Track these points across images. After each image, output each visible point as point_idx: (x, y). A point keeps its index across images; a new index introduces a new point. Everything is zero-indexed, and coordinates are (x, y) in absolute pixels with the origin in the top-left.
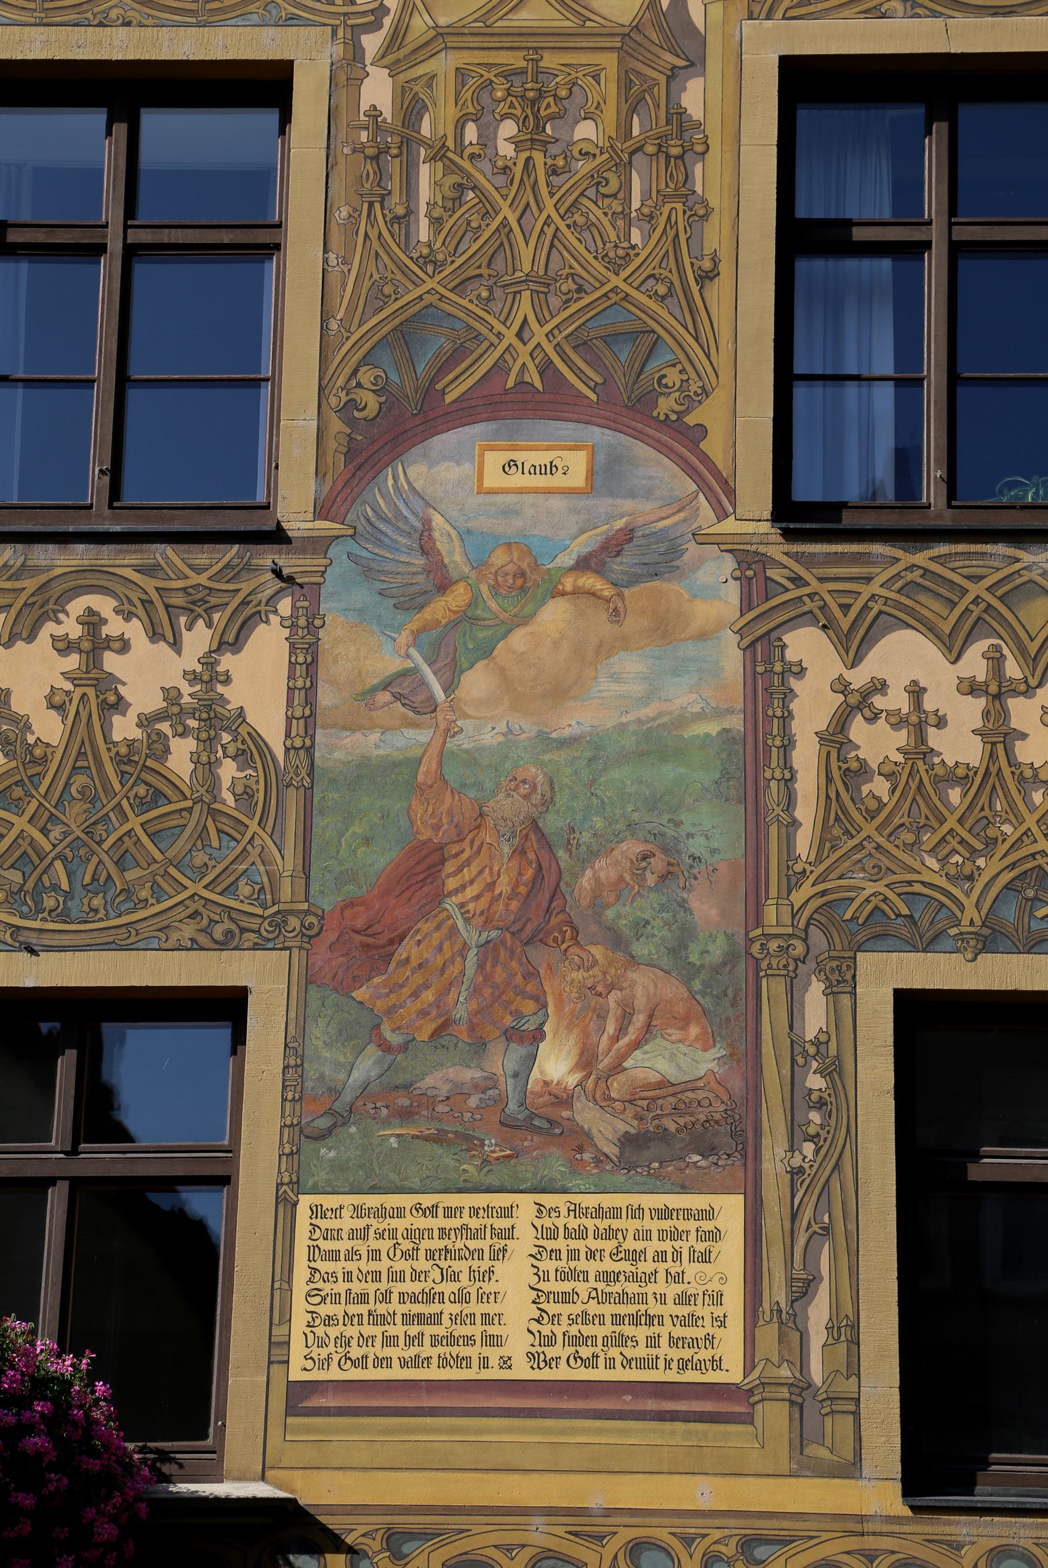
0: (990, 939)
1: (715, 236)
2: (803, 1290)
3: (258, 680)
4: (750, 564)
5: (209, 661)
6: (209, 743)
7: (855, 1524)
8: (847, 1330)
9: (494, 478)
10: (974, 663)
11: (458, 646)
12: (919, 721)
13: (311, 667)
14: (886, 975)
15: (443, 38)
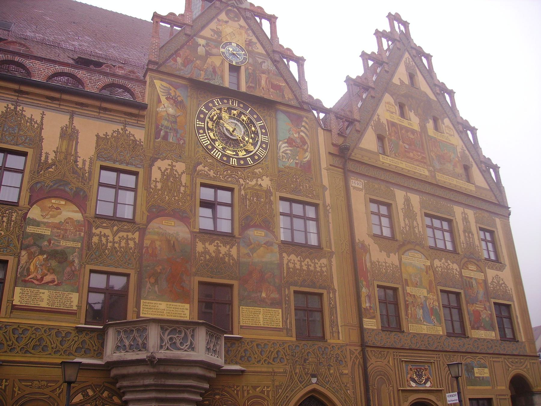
0: (301, 286)
1: (274, 212)
2: (287, 319)
3: (234, 251)
4: (279, 246)
5: (229, 249)
6: (229, 258)
7: (292, 341)
8: (291, 323)
9: (256, 234)
10: (299, 258)
11: (253, 250)
12: (294, 264)
13: (239, 251)
14: (293, 288)
15: (249, 188)
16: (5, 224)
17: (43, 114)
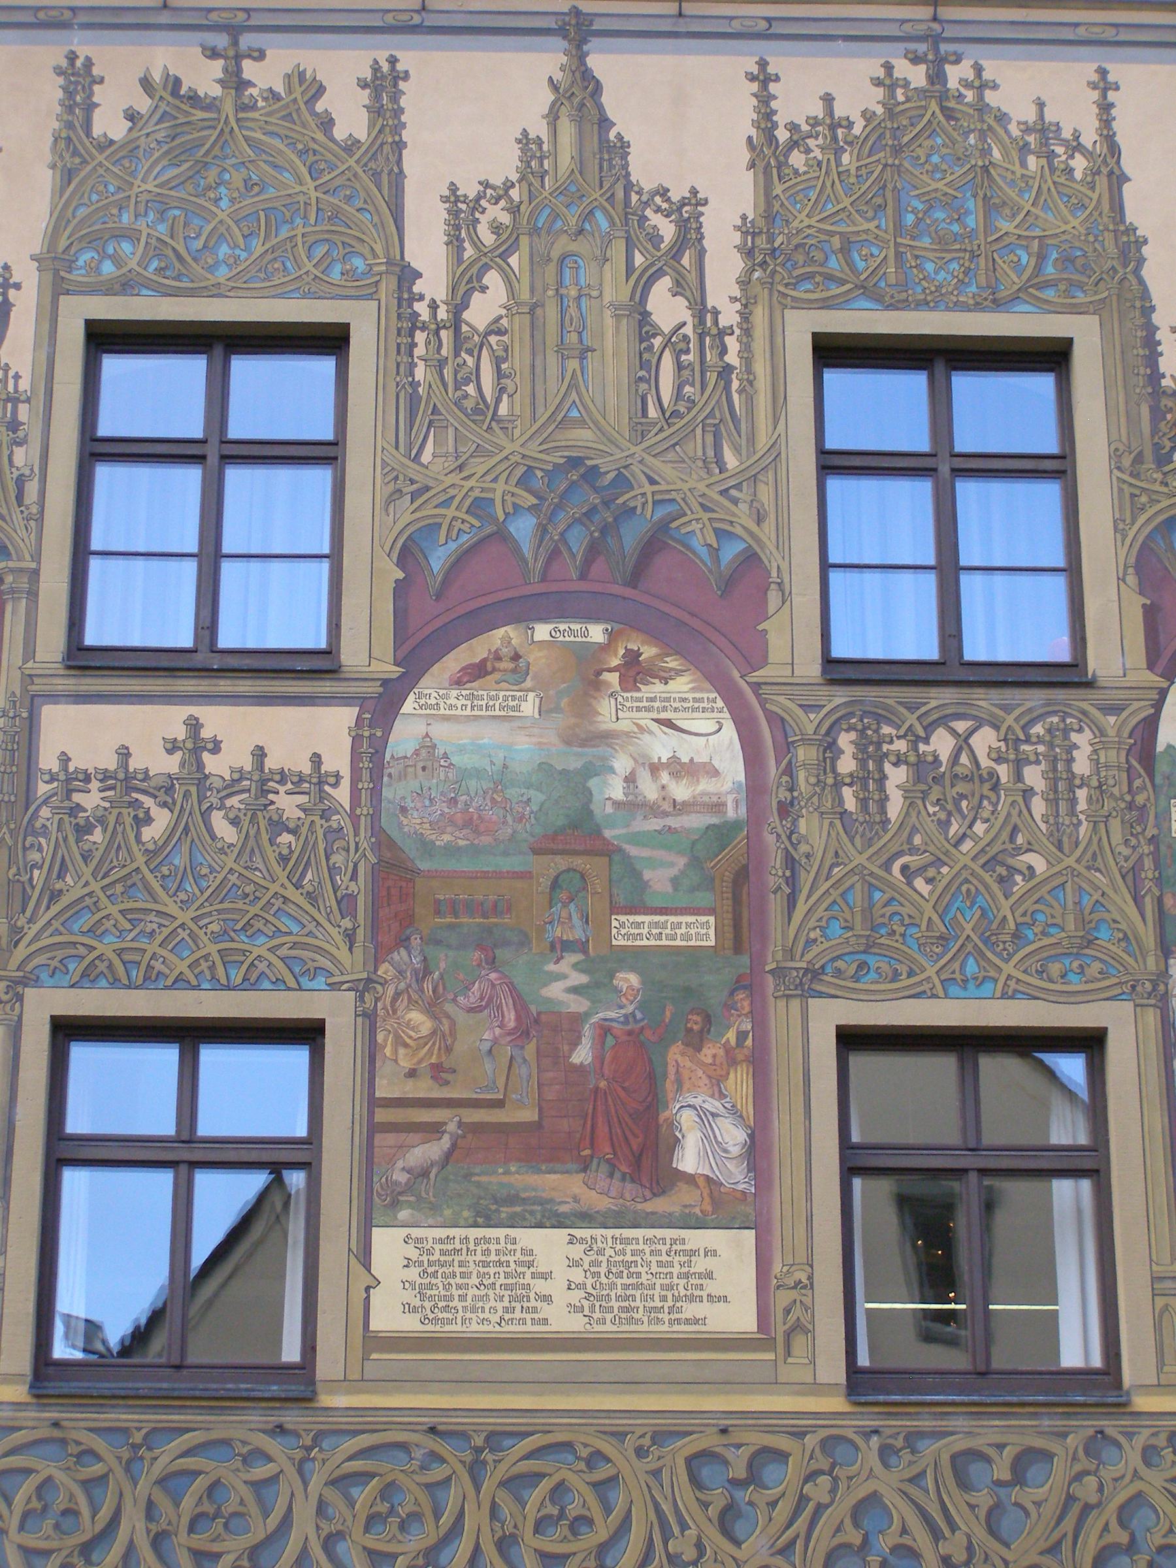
16: (1038, 806)
17: (1104, 85)
